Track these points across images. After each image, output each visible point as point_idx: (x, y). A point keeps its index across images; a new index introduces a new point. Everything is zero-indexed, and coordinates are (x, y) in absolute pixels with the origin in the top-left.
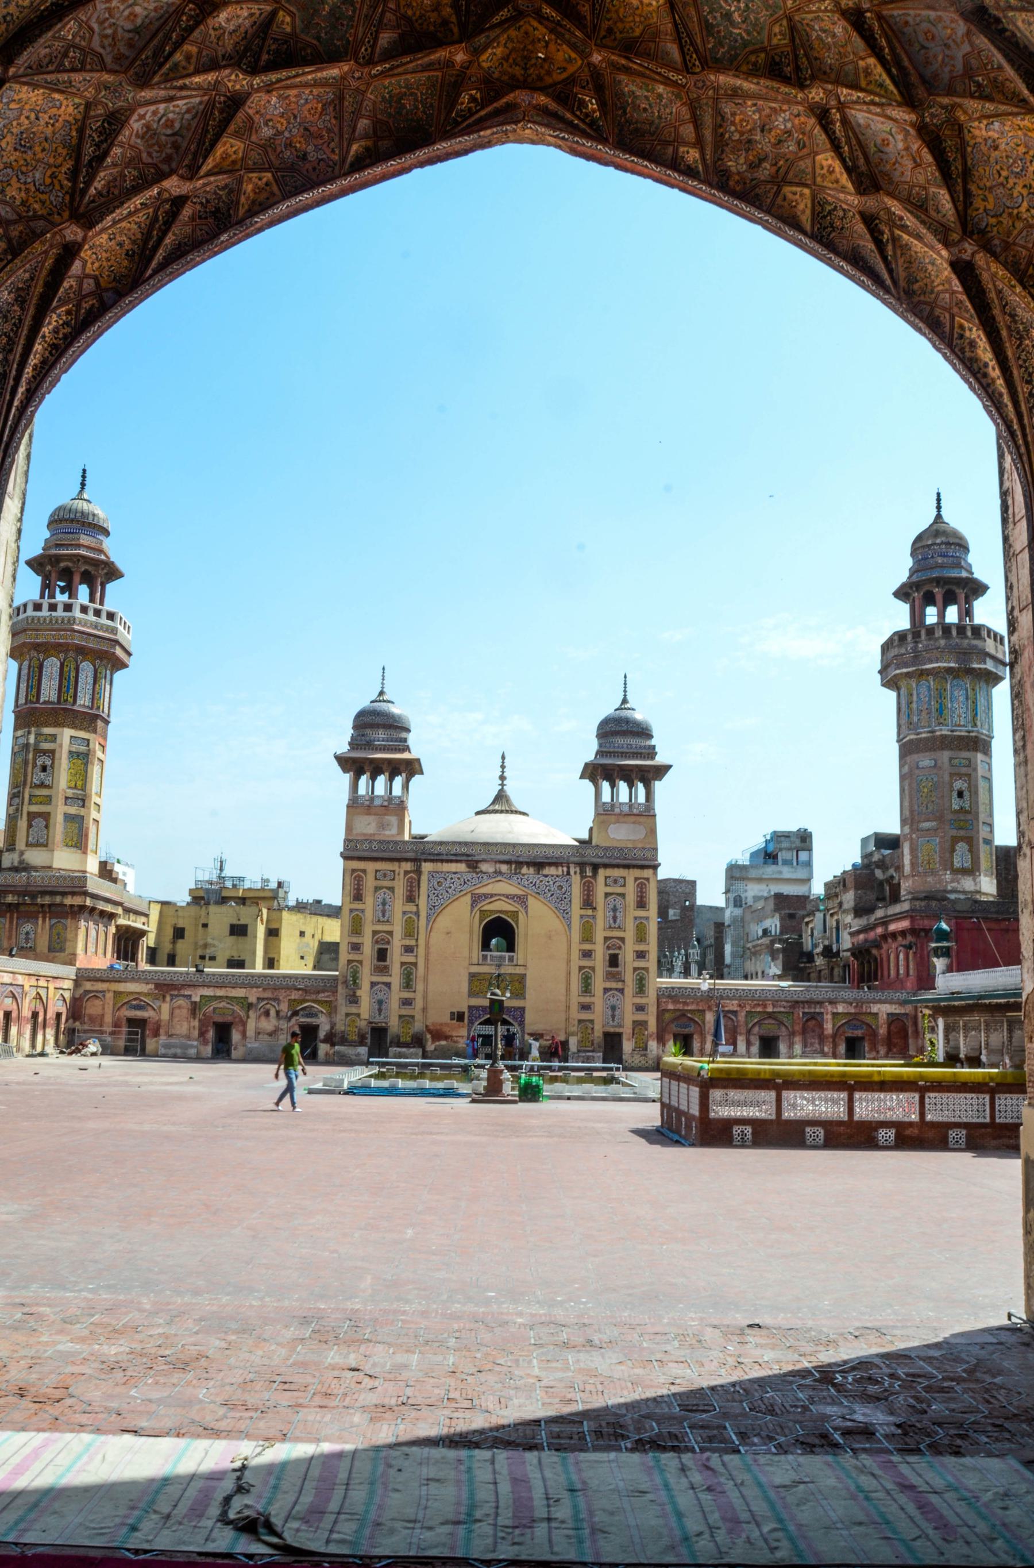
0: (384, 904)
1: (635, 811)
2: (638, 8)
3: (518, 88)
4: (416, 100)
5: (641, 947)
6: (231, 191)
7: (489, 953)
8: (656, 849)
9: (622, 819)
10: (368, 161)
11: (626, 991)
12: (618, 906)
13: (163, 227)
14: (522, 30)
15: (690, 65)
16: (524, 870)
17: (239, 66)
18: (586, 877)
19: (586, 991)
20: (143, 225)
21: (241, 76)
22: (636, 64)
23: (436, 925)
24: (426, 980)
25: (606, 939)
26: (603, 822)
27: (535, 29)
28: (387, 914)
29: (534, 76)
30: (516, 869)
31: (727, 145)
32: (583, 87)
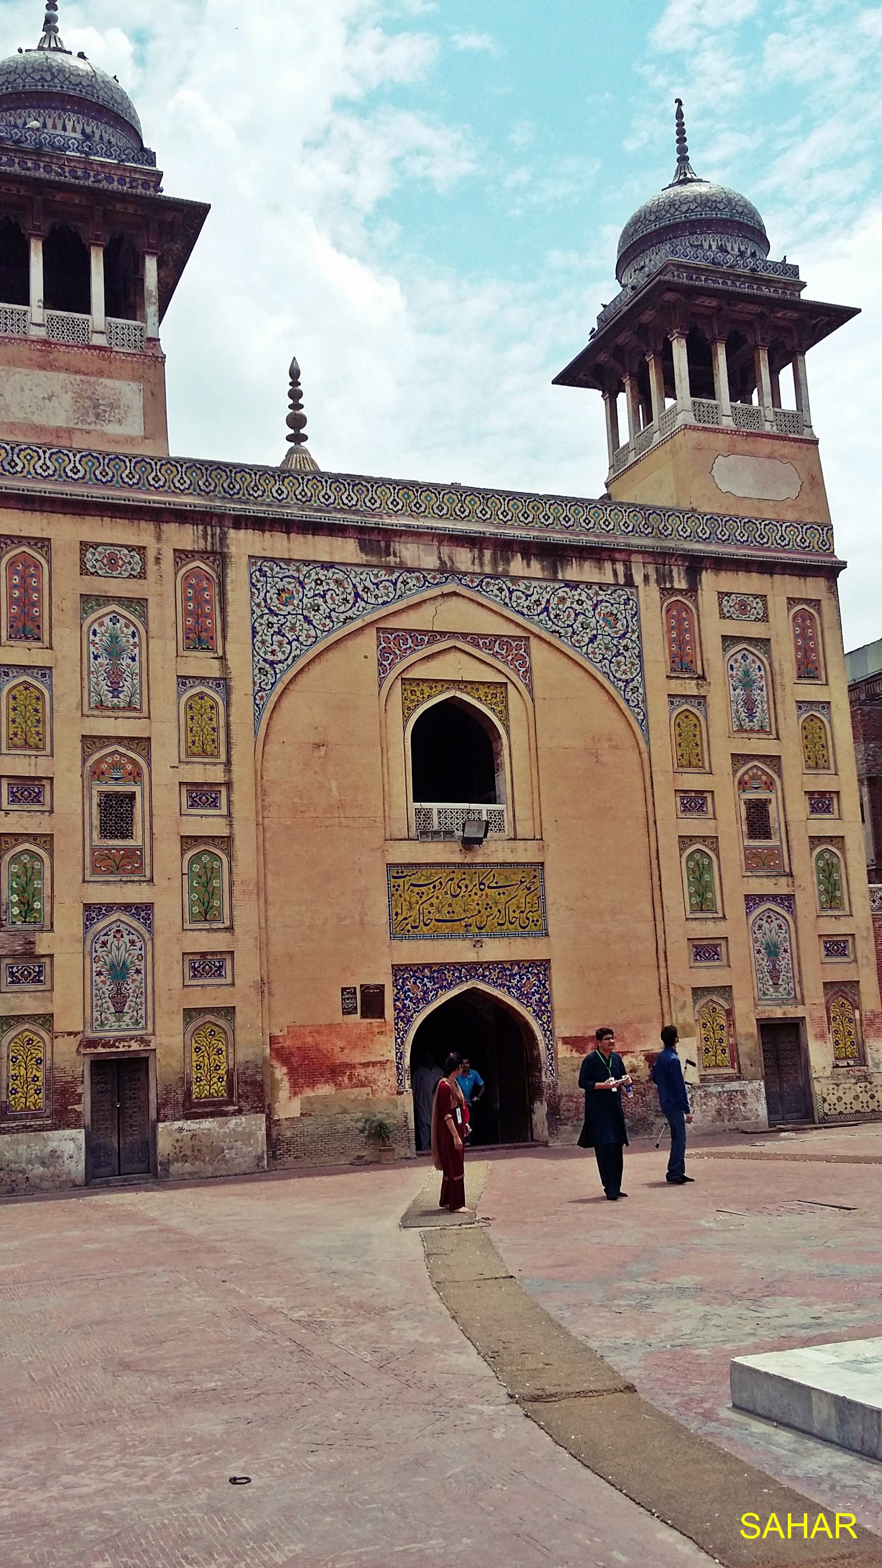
0: (114, 651)
1: (768, 428)
5: (823, 783)
7: (435, 806)
8: (827, 528)
9: (743, 445)
11: (799, 901)
12: (755, 674)
16: (517, 566)
18: (673, 591)
19: (700, 907)
23: (279, 721)
24: (261, 890)
25: (738, 759)
26: (698, 448)
28: (127, 687)
30: (494, 562)
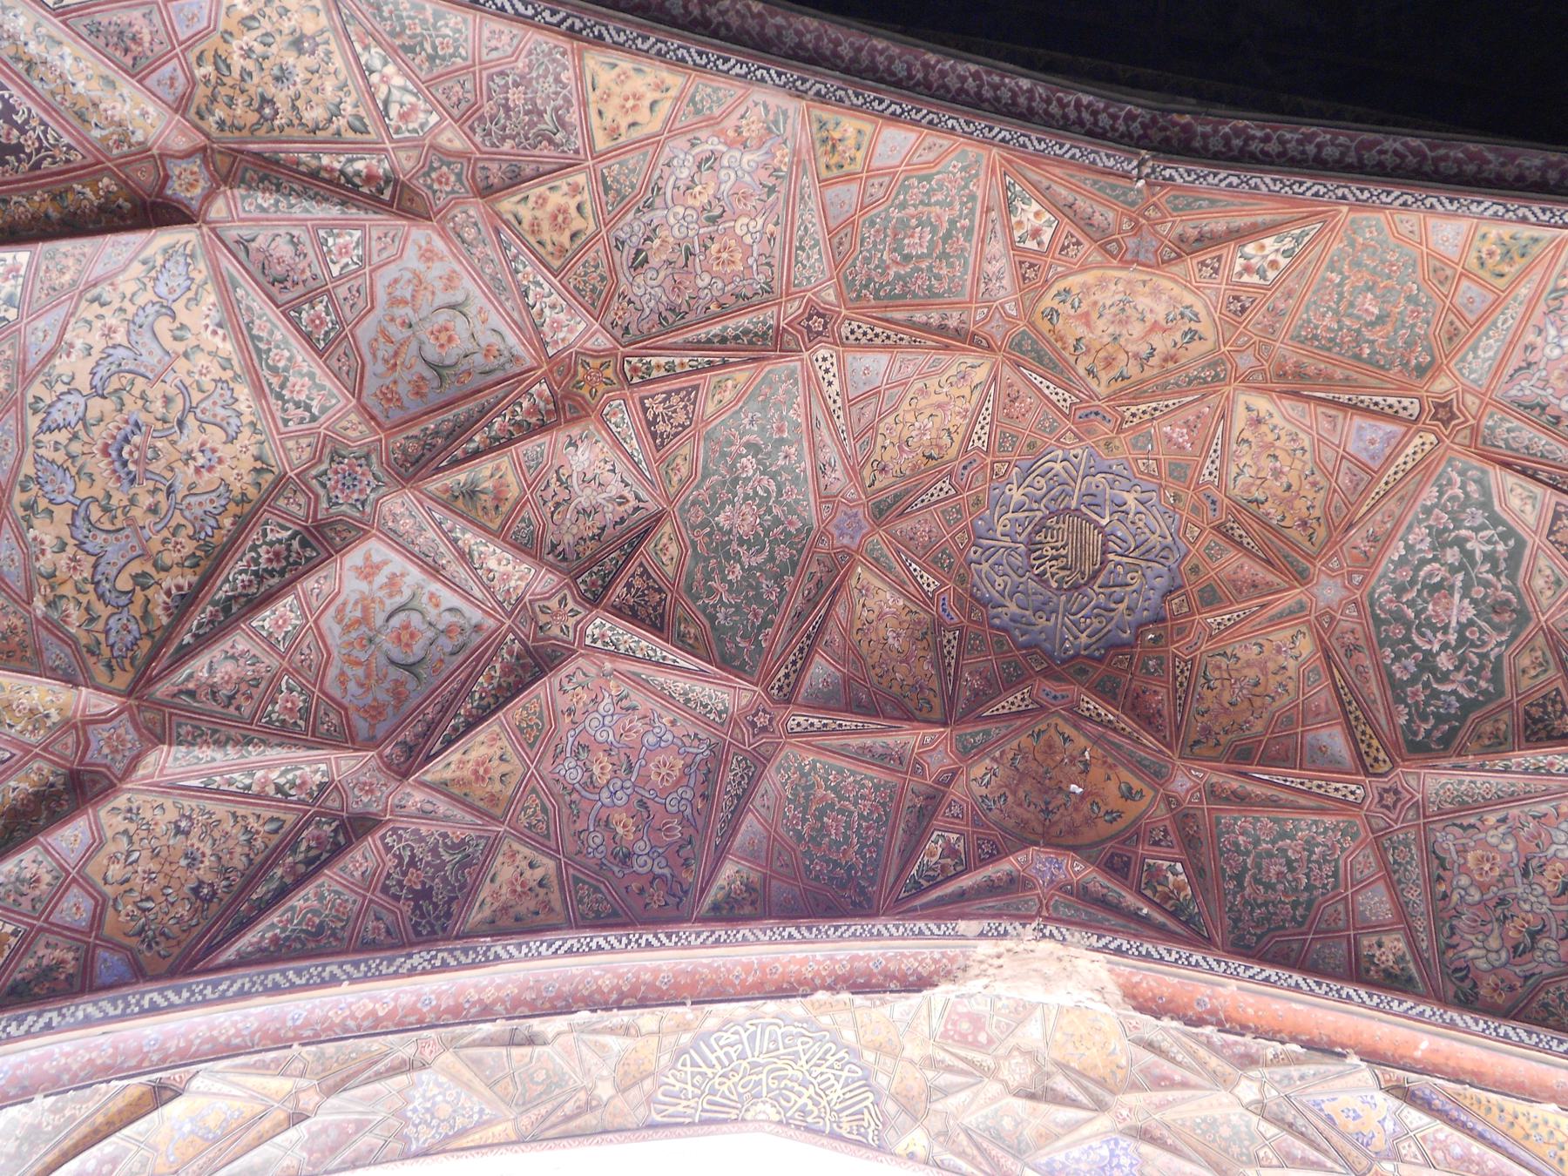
2: (1257, 684)
3: (1037, 844)
4: (849, 826)
6: (464, 864)
10: (747, 910)
13: (301, 868)
14: (1044, 737)
15: (1368, 761)
17: (575, 579)
20: (259, 844)
21: (571, 604)
22: (1262, 781)
27: (1066, 739)
29: (1061, 826)
31: (1459, 915)
32: (1157, 843)
